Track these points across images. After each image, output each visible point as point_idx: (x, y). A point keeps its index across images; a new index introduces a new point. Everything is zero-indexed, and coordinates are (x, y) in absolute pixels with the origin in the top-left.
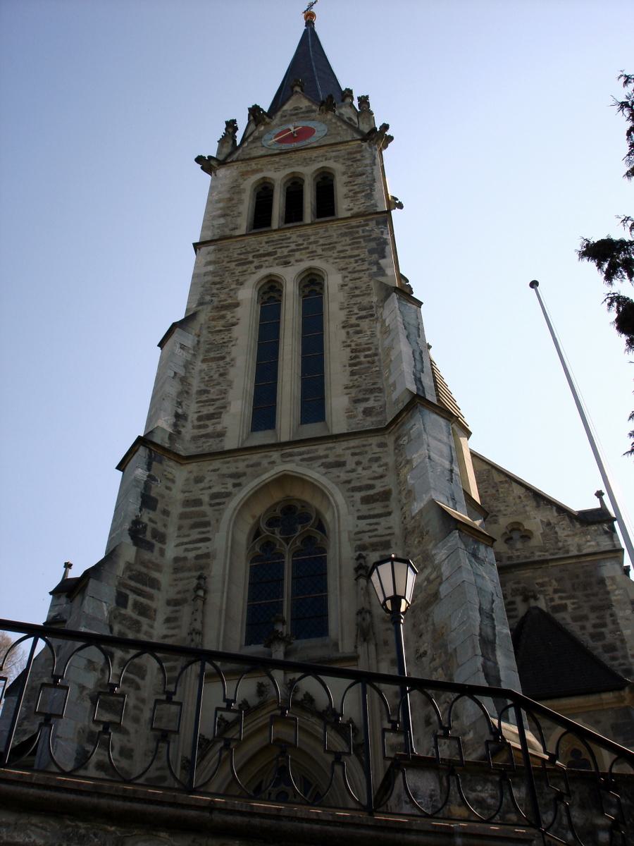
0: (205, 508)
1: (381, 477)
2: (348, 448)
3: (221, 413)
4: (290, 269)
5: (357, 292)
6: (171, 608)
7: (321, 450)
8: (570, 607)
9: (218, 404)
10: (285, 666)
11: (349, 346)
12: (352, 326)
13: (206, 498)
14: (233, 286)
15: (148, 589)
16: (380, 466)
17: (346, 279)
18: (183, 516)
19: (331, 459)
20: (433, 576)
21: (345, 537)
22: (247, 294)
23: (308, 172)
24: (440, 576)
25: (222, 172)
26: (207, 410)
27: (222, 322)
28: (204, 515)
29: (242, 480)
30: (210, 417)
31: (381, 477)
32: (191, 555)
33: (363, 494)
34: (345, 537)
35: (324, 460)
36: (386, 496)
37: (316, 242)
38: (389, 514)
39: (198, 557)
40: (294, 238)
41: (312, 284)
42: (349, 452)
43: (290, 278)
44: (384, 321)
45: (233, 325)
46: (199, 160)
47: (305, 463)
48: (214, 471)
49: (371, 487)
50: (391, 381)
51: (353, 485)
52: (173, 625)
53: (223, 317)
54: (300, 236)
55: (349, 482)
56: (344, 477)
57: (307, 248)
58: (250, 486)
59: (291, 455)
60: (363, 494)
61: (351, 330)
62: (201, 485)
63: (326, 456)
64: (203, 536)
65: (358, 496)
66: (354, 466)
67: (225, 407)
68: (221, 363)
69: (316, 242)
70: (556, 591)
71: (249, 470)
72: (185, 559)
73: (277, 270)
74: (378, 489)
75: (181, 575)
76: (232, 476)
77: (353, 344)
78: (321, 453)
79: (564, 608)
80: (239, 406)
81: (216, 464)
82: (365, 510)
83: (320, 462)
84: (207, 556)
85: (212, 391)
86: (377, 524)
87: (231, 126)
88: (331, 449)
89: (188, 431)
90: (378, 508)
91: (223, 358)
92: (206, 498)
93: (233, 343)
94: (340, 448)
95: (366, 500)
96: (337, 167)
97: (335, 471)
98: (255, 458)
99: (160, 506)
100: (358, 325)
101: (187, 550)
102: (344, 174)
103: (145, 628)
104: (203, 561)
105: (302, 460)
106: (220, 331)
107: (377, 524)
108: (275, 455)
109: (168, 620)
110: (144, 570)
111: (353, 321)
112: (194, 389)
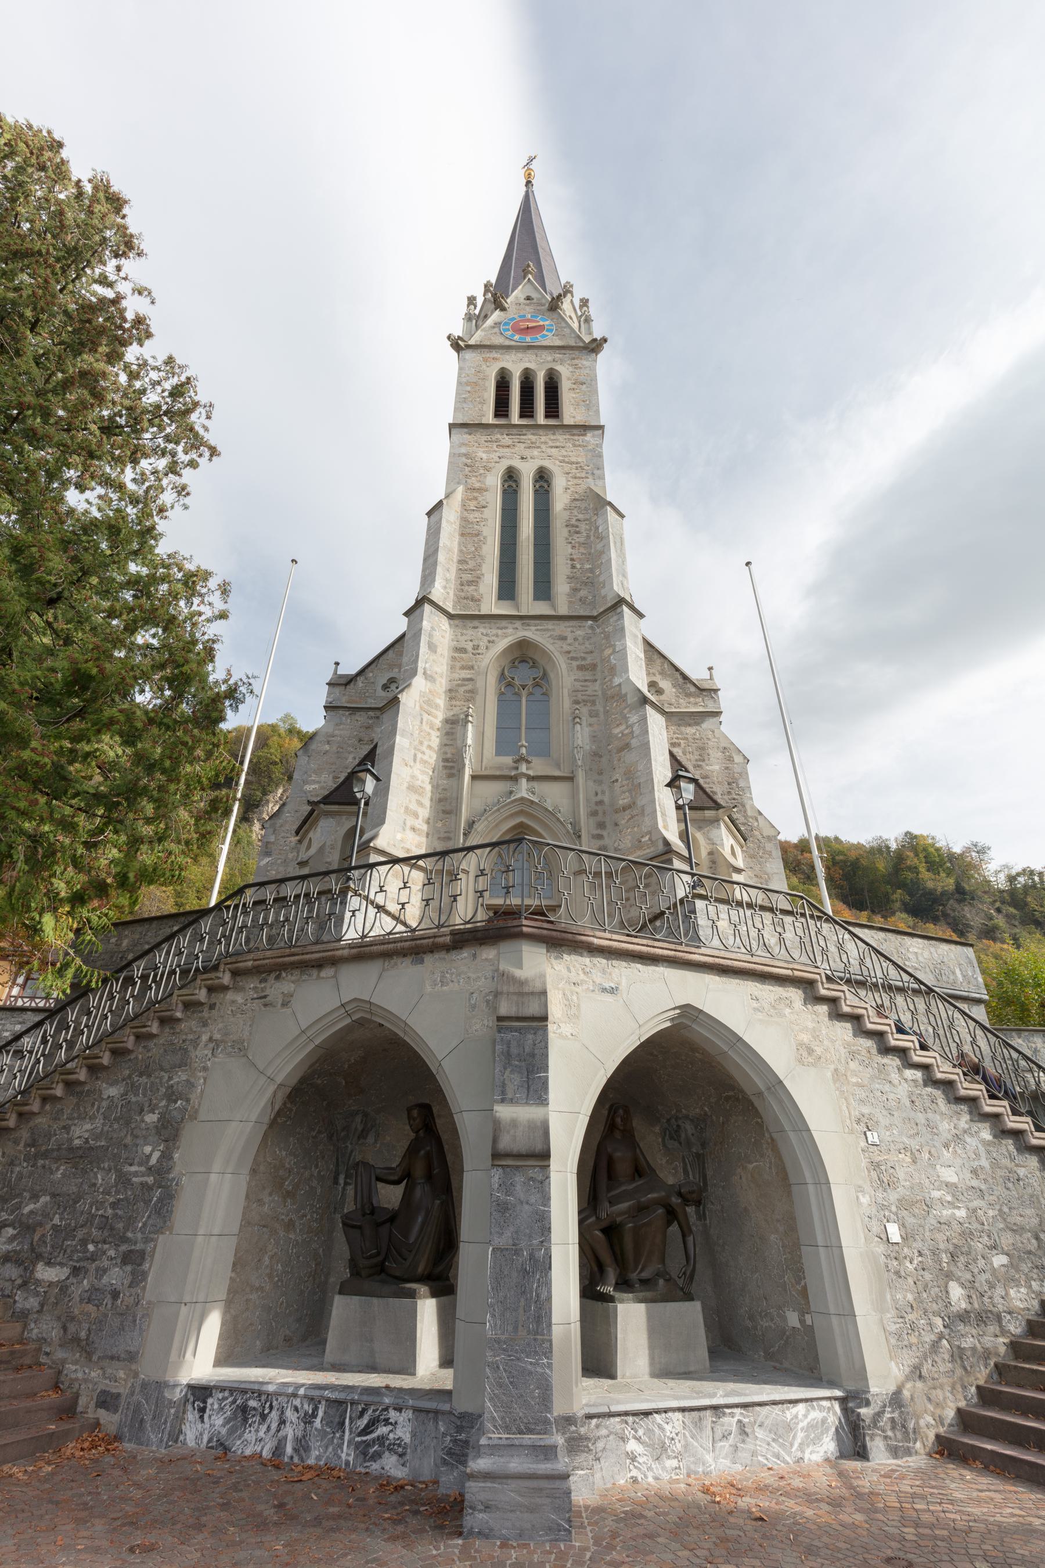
7: (549, 625)
8: (683, 745)
10: (530, 779)
12: (573, 526)
14: (482, 471)
15: (433, 711)
19: (557, 633)
20: (626, 732)
21: (566, 691)
24: (632, 732)
25: (468, 355)
26: (467, 577)
27: (475, 503)
30: (470, 583)
33: (578, 663)
34: (566, 691)
36: (594, 667)
37: (546, 443)
38: (596, 680)
41: (543, 477)
42: (569, 629)
44: (597, 528)
46: (449, 338)
49: (584, 659)
50: (601, 579)
55: (569, 652)
56: (566, 648)
57: (539, 447)
58: (503, 644)
60: (578, 663)
61: (573, 529)
63: (553, 630)
65: (575, 663)
68: (476, 539)
69: (546, 443)
70: (674, 733)
73: (517, 463)
74: (589, 661)
75: (454, 702)
78: (550, 627)
79: (679, 745)
80: (490, 579)
82: (580, 675)
83: (549, 634)
87: (471, 300)
90: (588, 675)
91: (477, 535)
94: (562, 628)
95: (581, 668)
97: (560, 643)
100: (577, 527)
102: (569, 379)
108: (518, 624)
110: (430, 696)
111: (573, 522)
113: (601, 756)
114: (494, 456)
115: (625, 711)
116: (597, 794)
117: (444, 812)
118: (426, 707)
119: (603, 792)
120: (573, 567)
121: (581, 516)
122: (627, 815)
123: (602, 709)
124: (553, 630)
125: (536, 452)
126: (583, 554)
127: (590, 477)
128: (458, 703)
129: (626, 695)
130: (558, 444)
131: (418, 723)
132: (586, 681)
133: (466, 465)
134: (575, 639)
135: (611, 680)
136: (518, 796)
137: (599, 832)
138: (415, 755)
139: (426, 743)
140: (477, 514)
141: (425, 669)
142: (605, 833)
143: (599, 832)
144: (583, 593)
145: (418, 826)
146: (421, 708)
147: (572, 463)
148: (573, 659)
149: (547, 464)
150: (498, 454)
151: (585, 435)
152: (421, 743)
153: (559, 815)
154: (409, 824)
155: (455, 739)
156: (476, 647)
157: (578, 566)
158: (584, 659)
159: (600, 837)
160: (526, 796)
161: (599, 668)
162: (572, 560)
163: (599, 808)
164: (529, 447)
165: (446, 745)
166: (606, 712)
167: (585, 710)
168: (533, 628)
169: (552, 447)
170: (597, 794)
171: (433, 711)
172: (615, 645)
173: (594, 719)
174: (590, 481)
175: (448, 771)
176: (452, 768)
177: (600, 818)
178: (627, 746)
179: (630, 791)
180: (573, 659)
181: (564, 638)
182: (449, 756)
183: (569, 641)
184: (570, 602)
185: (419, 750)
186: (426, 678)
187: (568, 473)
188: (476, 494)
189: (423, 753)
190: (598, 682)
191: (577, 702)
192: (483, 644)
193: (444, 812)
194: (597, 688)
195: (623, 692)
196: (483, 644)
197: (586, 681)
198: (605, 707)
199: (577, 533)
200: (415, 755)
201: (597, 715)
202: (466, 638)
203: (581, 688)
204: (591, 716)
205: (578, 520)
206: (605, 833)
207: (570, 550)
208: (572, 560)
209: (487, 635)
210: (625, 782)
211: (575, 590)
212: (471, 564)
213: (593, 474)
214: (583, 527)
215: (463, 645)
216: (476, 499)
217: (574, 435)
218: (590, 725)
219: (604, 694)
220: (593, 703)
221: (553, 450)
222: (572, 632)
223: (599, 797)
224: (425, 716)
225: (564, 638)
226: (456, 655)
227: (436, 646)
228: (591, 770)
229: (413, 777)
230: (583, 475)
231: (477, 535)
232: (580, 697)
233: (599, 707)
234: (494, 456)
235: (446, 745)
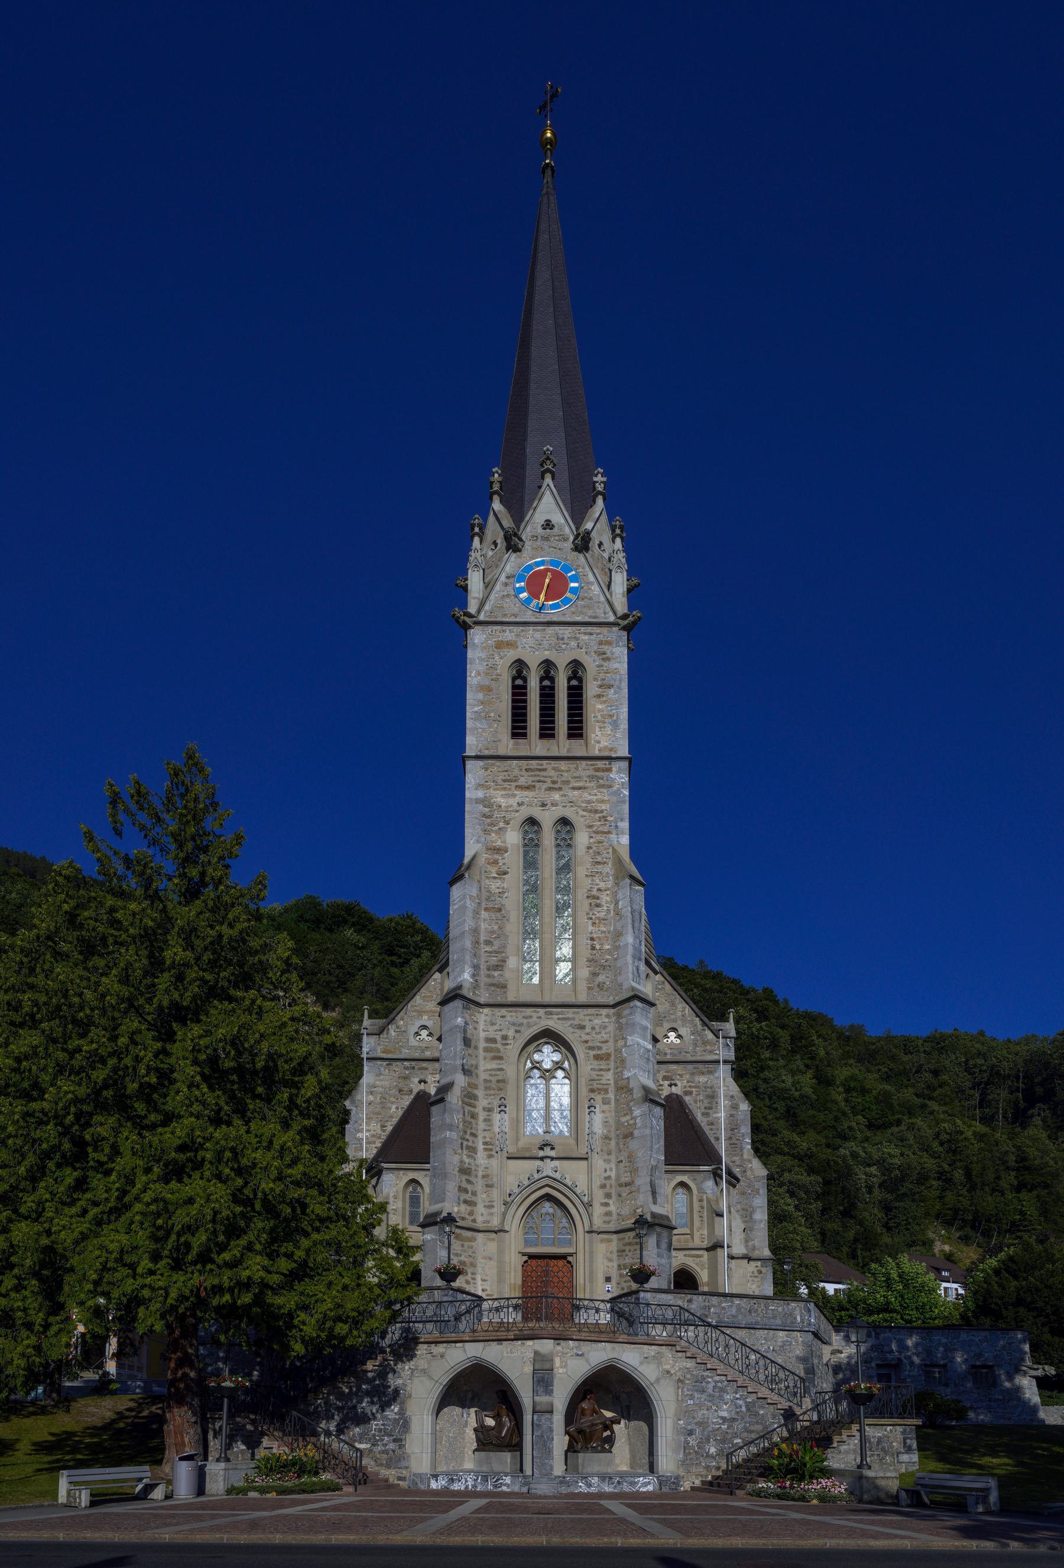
0: (499, 1046)
1: (607, 1042)
2: (588, 1015)
3: (503, 966)
4: (547, 813)
5: (599, 859)
6: (486, 1113)
7: (569, 1013)
9: (500, 956)
11: (591, 918)
13: (499, 1038)
14: (502, 825)
16: (606, 1034)
17: (592, 840)
18: (486, 1050)
19: (576, 1022)
22: (513, 838)
23: (562, 661)
26: (494, 960)
28: (498, 1050)
29: (522, 1029)
31: (607, 1042)
32: (493, 1079)
33: (595, 1052)
35: (572, 1022)
37: (568, 782)
38: (609, 1070)
39: (498, 1081)
40: (552, 773)
42: (588, 1018)
43: (547, 819)
45: (505, 873)
47: (560, 1022)
48: (503, 1017)
49: (600, 1048)
51: (590, 1044)
52: (488, 1123)
53: (496, 862)
54: (554, 769)
55: (586, 1042)
56: (585, 1037)
57: (560, 789)
59: (551, 1014)
60: (595, 1052)
62: (496, 1027)
63: (573, 1019)
64: (500, 1067)
65: (592, 1053)
66: (590, 1030)
67: (505, 961)
68: (498, 915)
71: (525, 1021)
72: (490, 1081)
73: (537, 813)
75: (489, 1092)
76: (514, 1024)
77: (594, 917)
78: (570, 1016)
81: (504, 1011)
82: (595, 1064)
83: (570, 1023)
84: (503, 1081)
85: (495, 943)
86: (601, 1076)
88: (578, 1013)
89: (483, 980)
92: (499, 1038)
93: (506, 895)
95: (597, 1057)
96: (590, 663)
98: (529, 1011)
99: (473, 1044)
100: (598, 898)
101: (491, 1075)
103: (474, 1125)
104: (501, 1085)
105: (559, 1019)
106: (495, 878)
107: (601, 1076)
108: (541, 1011)
109: (485, 1120)
111: (595, 892)
112: (482, 938)
113: (610, 1139)
114: (513, 802)
115: (631, 1104)
116: (606, 1171)
117: (487, 1186)
118: (466, 1100)
119: (611, 1170)
120: (593, 948)
121: (602, 885)
122: (627, 1189)
123: (613, 1097)
124: (573, 1019)
125: (556, 796)
126: (603, 932)
127: (614, 832)
128: (492, 1092)
129: (632, 1090)
130: (581, 784)
131: (461, 1116)
132: (601, 1070)
133: (484, 816)
134: (593, 1028)
135: (621, 1072)
136: (544, 1174)
137: (606, 1200)
138: (462, 1144)
139: (469, 1132)
140: (499, 883)
141: (463, 1065)
142: (611, 1202)
143: (606, 1200)
144: (601, 978)
145: (469, 1199)
146: (463, 1102)
147: (596, 811)
148: (591, 1048)
149: (569, 813)
150: (518, 799)
151: (609, 770)
152: (465, 1132)
153: (576, 1190)
154: (462, 1199)
155: (491, 1125)
156: (505, 1038)
157: (598, 947)
158: (600, 1048)
159: (607, 1204)
160: (551, 1174)
161: (612, 1058)
162: (592, 939)
163: (608, 1182)
164: (550, 789)
165: (485, 1130)
166: (617, 1100)
167: (599, 1098)
168: (556, 1017)
169: (574, 788)
170: (606, 1171)
171: (472, 1101)
172: (626, 1039)
173: (606, 1107)
174: (613, 836)
175: (487, 1153)
176: (491, 1150)
177: (607, 1190)
178: (631, 1134)
179: (631, 1172)
180: (591, 1048)
181: (582, 1027)
182: (488, 1140)
183: (588, 1030)
184: (589, 988)
185: (464, 1139)
186: (464, 1074)
187: (590, 827)
188: (496, 857)
189: (468, 1140)
190: (612, 1071)
191: (592, 1091)
192: (511, 1033)
193: (487, 1186)
194: (609, 1077)
195: (631, 1086)
196: (511, 1033)
197: (601, 1070)
198: (615, 1096)
199: (598, 906)
200: (462, 1144)
201: (608, 1103)
202: (496, 1027)
203: (596, 1078)
204: (604, 1104)
205: (599, 890)
206: (611, 1202)
207: (590, 928)
208: (592, 939)
209: (514, 1024)
210: (627, 1164)
211: (595, 974)
212: (497, 944)
213: (617, 827)
214: (605, 898)
215: (492, 1035)
216: (496, 862)
217: (597, 770)
218: (603, 1112)
219: (616, 1083)
220: (606, 1091)
221: (576, 793)
222: (590, 1020)
223: (608, 1173)
224: (467, 1108)
225: (582, 1027)
226: (488, 1045)
227: (470, 1040)
228: (602, 1151)
229: (461, 1162)
230: (606, 828)
231: (500, 910)
232: (595, 1086)
233: (611, 1095)
234: (513, 802)
235: (485, 1130)
